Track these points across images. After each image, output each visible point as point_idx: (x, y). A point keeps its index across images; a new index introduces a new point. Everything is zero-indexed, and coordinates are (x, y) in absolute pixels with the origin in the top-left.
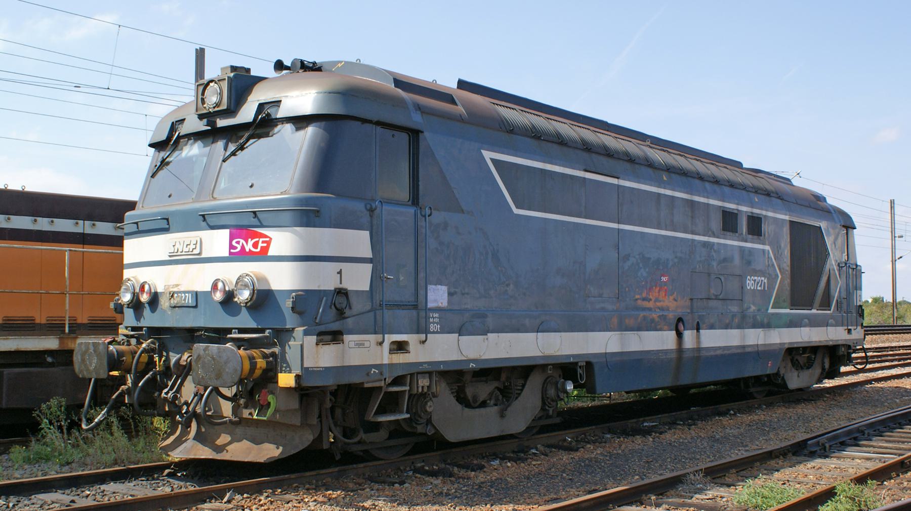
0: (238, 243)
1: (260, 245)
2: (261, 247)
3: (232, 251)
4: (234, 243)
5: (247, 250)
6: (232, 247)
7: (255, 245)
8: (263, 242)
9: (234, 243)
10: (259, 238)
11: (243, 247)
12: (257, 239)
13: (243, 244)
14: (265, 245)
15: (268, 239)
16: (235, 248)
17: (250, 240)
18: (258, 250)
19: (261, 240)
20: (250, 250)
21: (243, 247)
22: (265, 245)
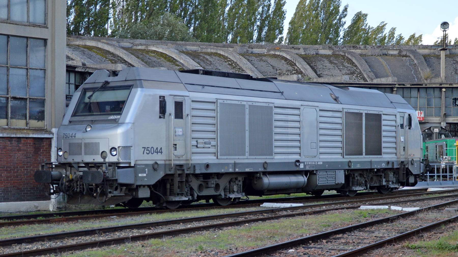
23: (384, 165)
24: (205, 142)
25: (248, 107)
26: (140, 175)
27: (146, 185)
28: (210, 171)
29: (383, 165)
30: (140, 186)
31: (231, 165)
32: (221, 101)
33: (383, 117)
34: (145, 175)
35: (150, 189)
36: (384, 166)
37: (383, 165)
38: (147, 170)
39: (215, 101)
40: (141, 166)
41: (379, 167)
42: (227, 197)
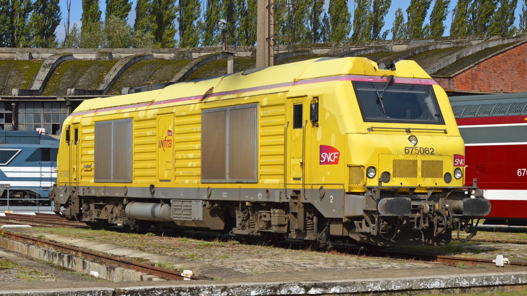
0: (324, 155)
1: (335, 157)
2: (335, 158)
3: (321, 161)
5: (329, 161)
6: (321, 159)
7: (332, 158)
8: (336, 155)
10: (334, 152)
11: (326, 158)
12: (333, 153)
14: (337, 157)
15: (338, 153)
16: (323, 159)
17: (330, 153)
18: (334, 161)
19: (335, 153)
20: (330, 160)
21: (326, 158)
22: (337, 157)
23: (261, 195)
29: (260, 196)
36: (260, 197)
37: (260, 196)
41: (252, 199)
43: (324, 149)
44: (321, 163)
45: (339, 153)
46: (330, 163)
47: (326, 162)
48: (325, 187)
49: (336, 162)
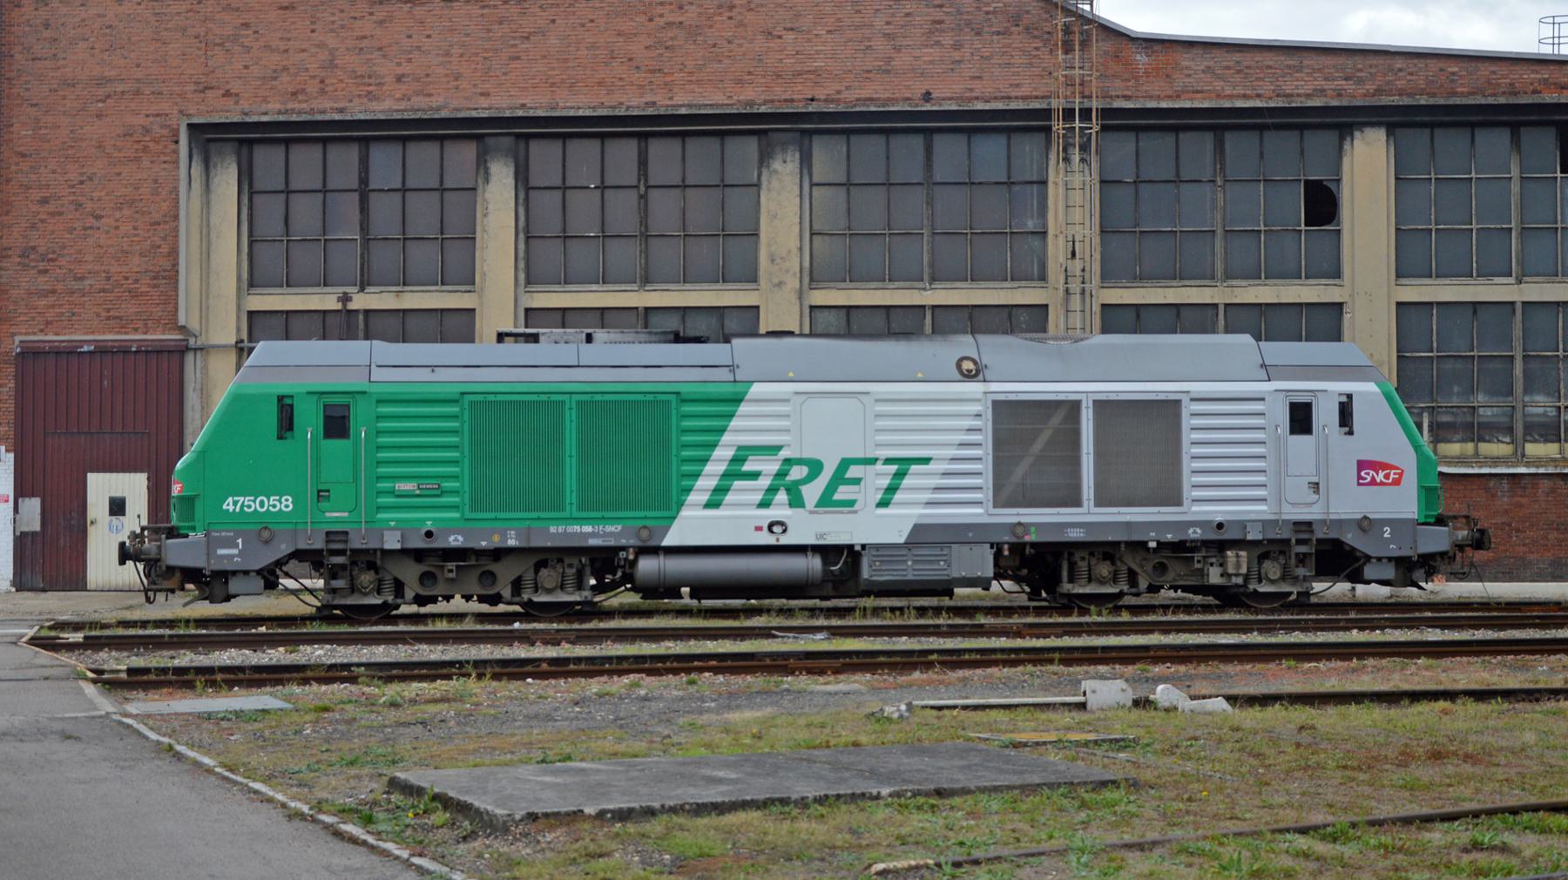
0: (1368, 474)
1: (1392, 476)
4: (1363, 474)
5: (1378, 481)
6: (1360, 477)
7: (1387, 477)
8: (1395, 474)
9: (1363, 474)
11: (1373, 478)
13: (1373, 476)
16: (1365, 479)
18: (1390, 481)
21: (1373, 478)
24: (419, 485)
25: (574, 406)
26: (221, 552)
27: (253, 571)
28: (437, 544)
30: (234, 573)
31: (513, 532)
32: (472, 397)
33: (1188, 408)
34: (235, 551)
35: (264, 577)
38: (240, 541)
39: (457, 397)
40: (223, 534)
42: (526, 600)
43: (1362, 465)
44: (1359, 484)
45: (1403, 471)
46: (1382, 484)
47: (1373, 482)
48: (1371, 516)
49: (1397, 482)
